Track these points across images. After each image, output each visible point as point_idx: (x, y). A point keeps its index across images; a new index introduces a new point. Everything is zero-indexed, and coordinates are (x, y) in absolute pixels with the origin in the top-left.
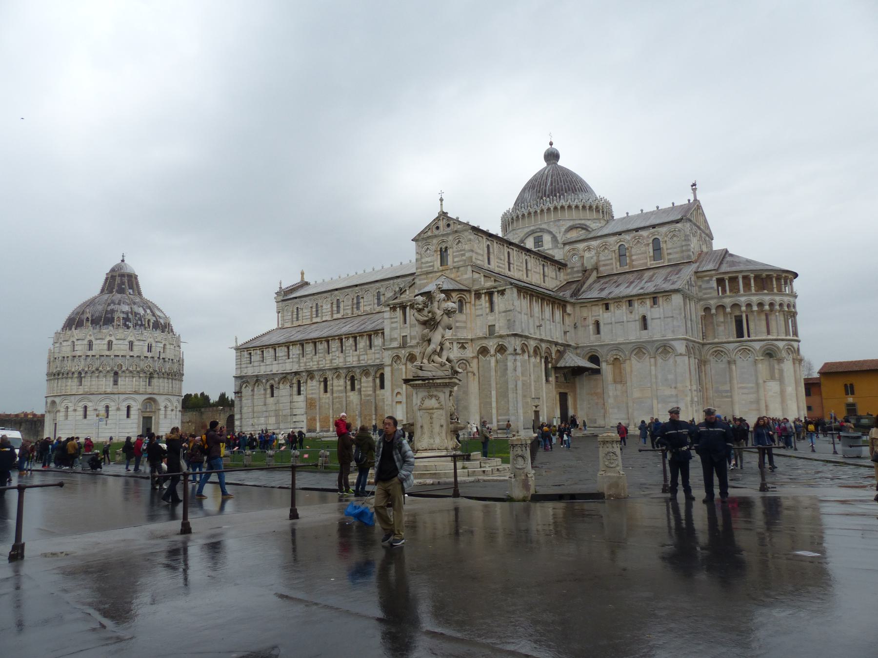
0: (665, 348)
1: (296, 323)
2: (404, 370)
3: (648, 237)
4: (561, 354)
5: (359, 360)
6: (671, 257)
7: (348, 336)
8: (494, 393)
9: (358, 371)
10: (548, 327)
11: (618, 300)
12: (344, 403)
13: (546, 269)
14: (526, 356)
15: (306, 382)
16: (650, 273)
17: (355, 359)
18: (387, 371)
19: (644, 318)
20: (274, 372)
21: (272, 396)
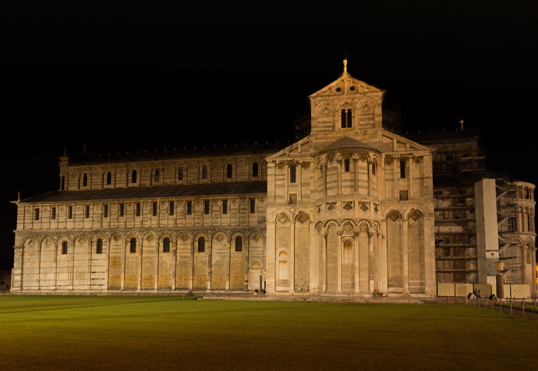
2: (292, 228)
5: (176, 224)
8: (406, 257)
9: (175, 233)
12: (156, 263)
21: (65, 252)
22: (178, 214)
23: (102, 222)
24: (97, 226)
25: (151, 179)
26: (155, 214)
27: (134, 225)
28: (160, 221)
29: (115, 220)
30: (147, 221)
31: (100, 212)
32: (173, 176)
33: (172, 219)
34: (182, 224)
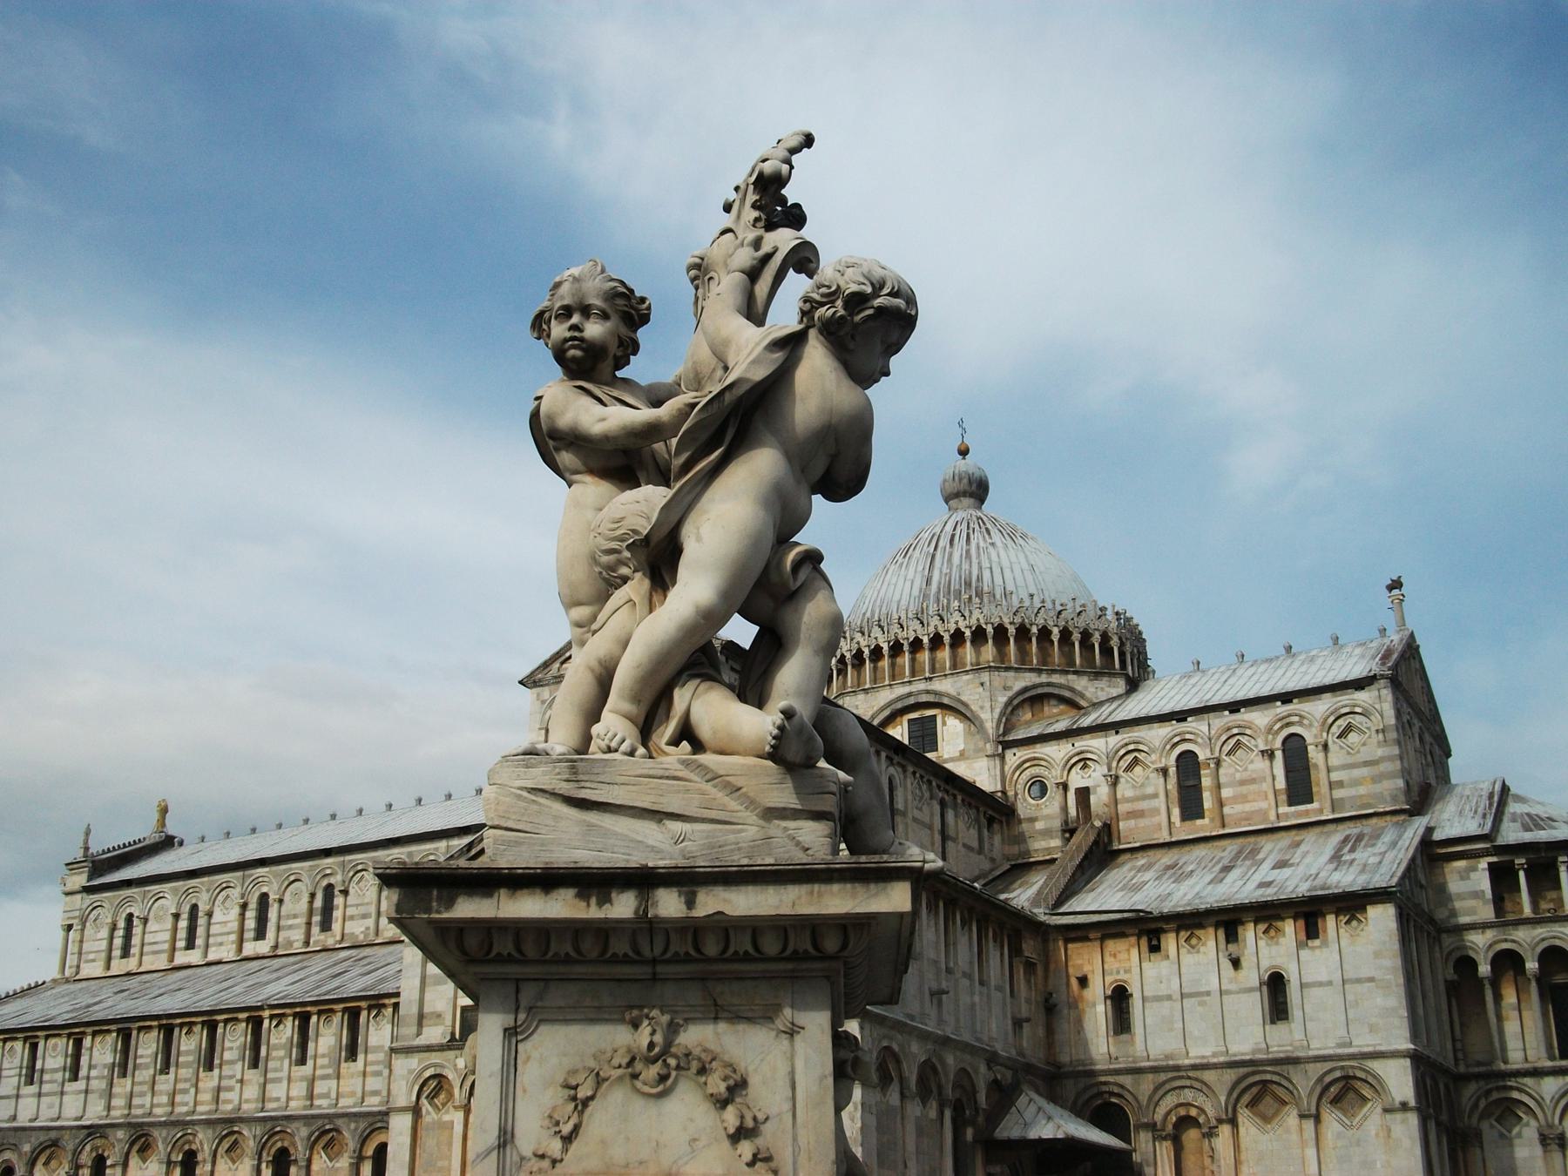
0: (1345, 1087)
1: (118, 966)
2: (458, 1129)
3: (1269, 730)
4: (1004, 1096)
5: (311, 1096)
6: (1339, 794)
7: (280, 1010)
10: (965, 999)
11: (1189, 922)
13: (950, 815)
14: (894, 1097)
15: (125, 1165)
16: (1285, 839)
17: (299, 1090)
18: (399, 1130)
19: (1276, 984)
20: (23, 1121)
22: (320, 1061)
23: (110, 1096)
24: (95, 1113)
25: (309, 924)
26: (255, 1064)
27: (196, 1104)
28: (269, 1087)
29: (145, 1088)
30: (230, 1089)
31: (109, 1058)
32: (373, 909)
33: (302, 1079)
34: (326, 1096)
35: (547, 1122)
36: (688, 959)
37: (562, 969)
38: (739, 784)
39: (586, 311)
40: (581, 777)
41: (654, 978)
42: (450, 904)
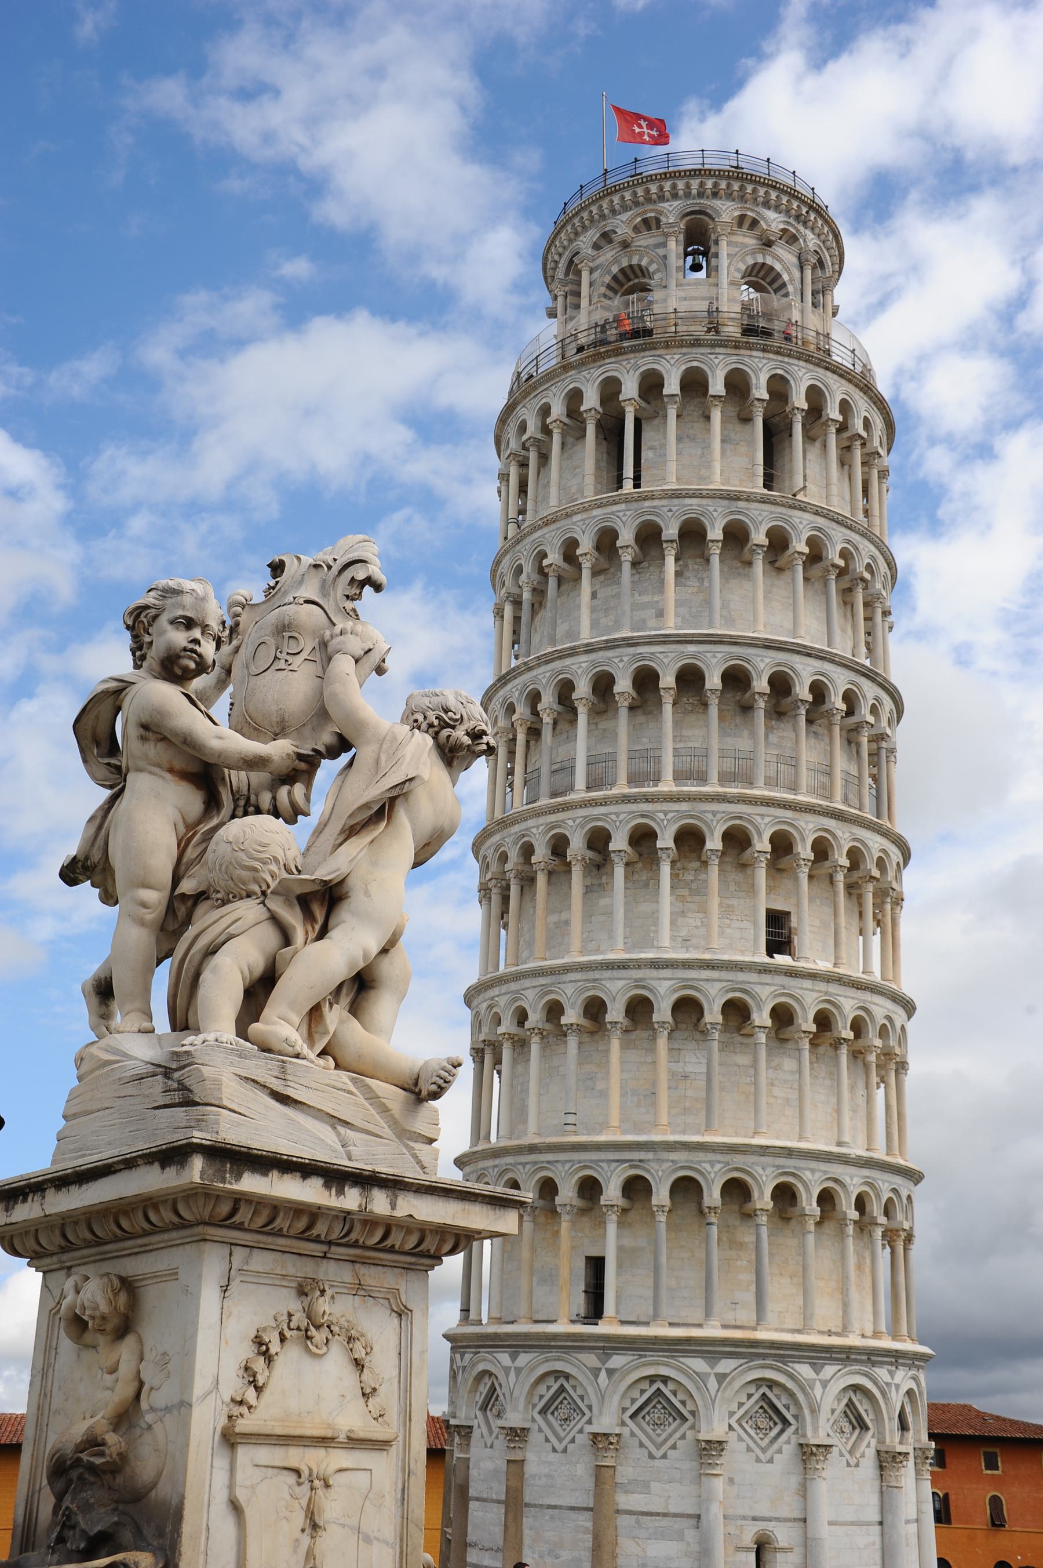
35: (241, 1372)
36: (355, 1245)
37: (270, 1239)
38: (390, 1107)
39: (205, 628)
40: (288, 1077)
41: (324, 1257)
42: (238, 1177)
